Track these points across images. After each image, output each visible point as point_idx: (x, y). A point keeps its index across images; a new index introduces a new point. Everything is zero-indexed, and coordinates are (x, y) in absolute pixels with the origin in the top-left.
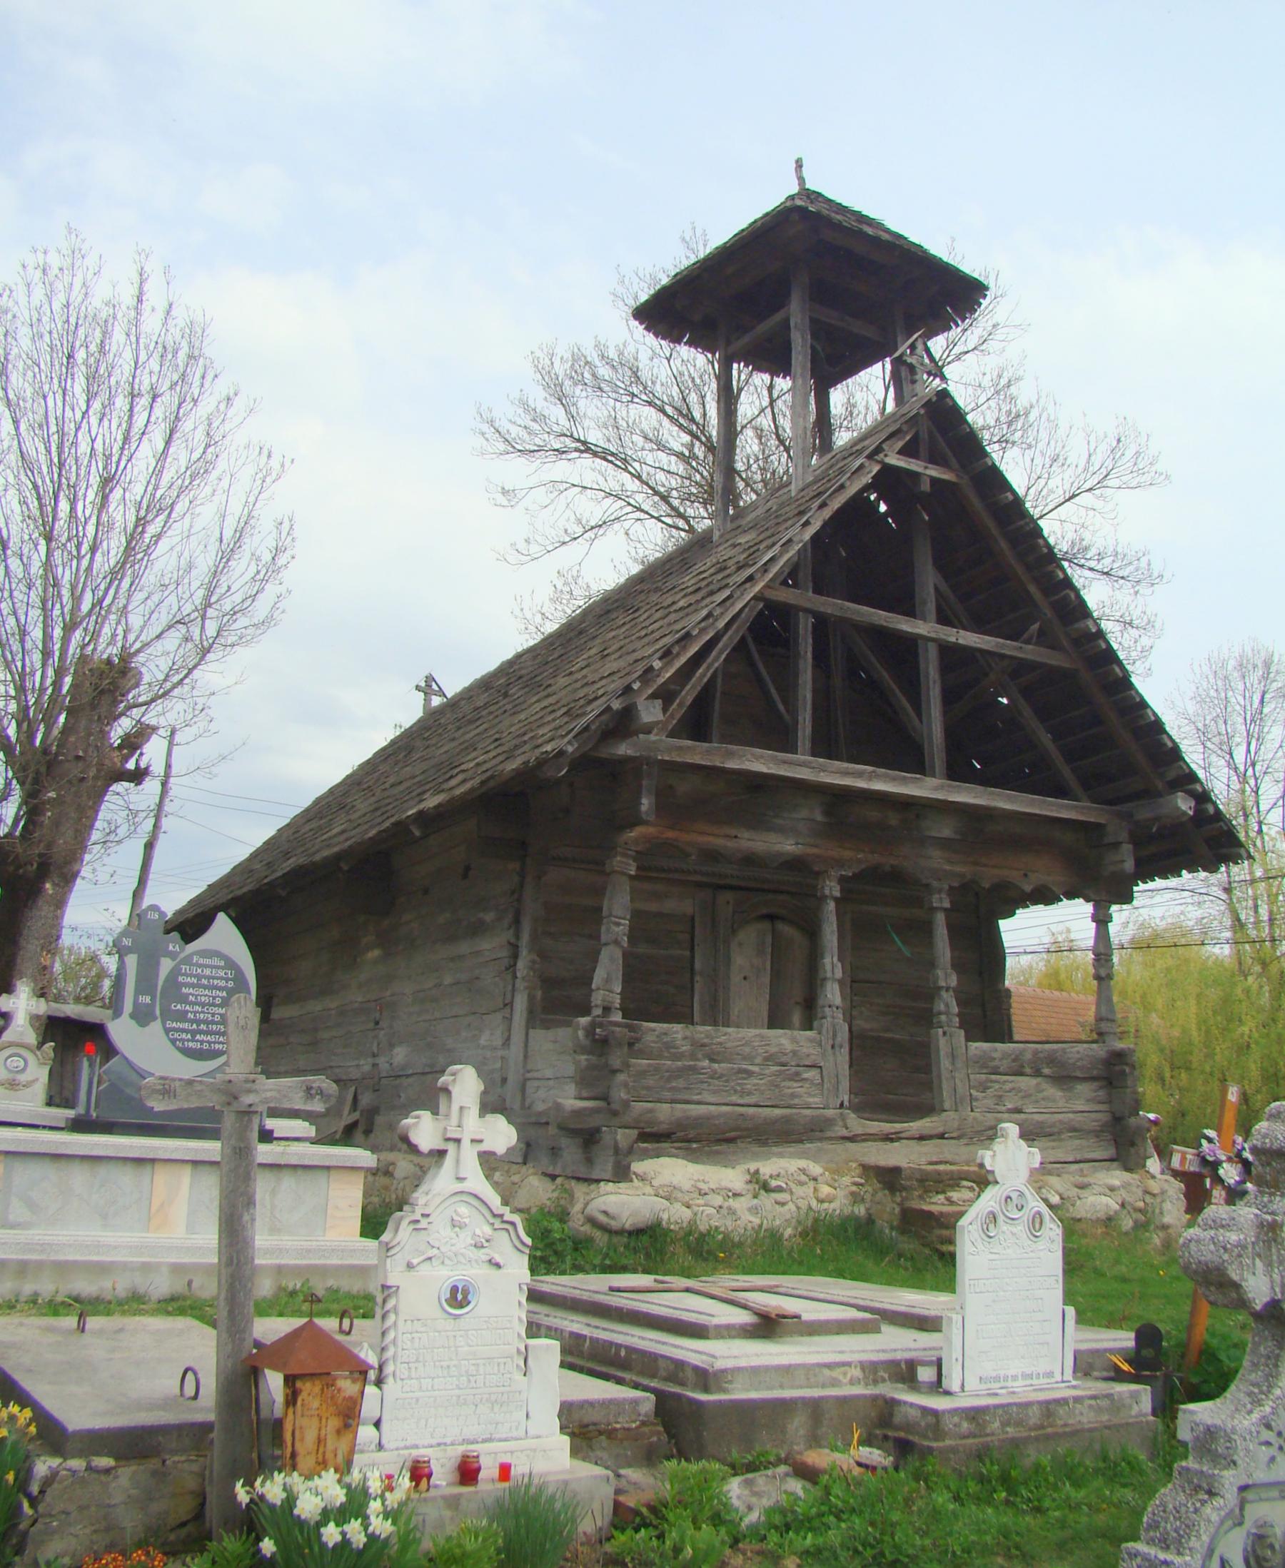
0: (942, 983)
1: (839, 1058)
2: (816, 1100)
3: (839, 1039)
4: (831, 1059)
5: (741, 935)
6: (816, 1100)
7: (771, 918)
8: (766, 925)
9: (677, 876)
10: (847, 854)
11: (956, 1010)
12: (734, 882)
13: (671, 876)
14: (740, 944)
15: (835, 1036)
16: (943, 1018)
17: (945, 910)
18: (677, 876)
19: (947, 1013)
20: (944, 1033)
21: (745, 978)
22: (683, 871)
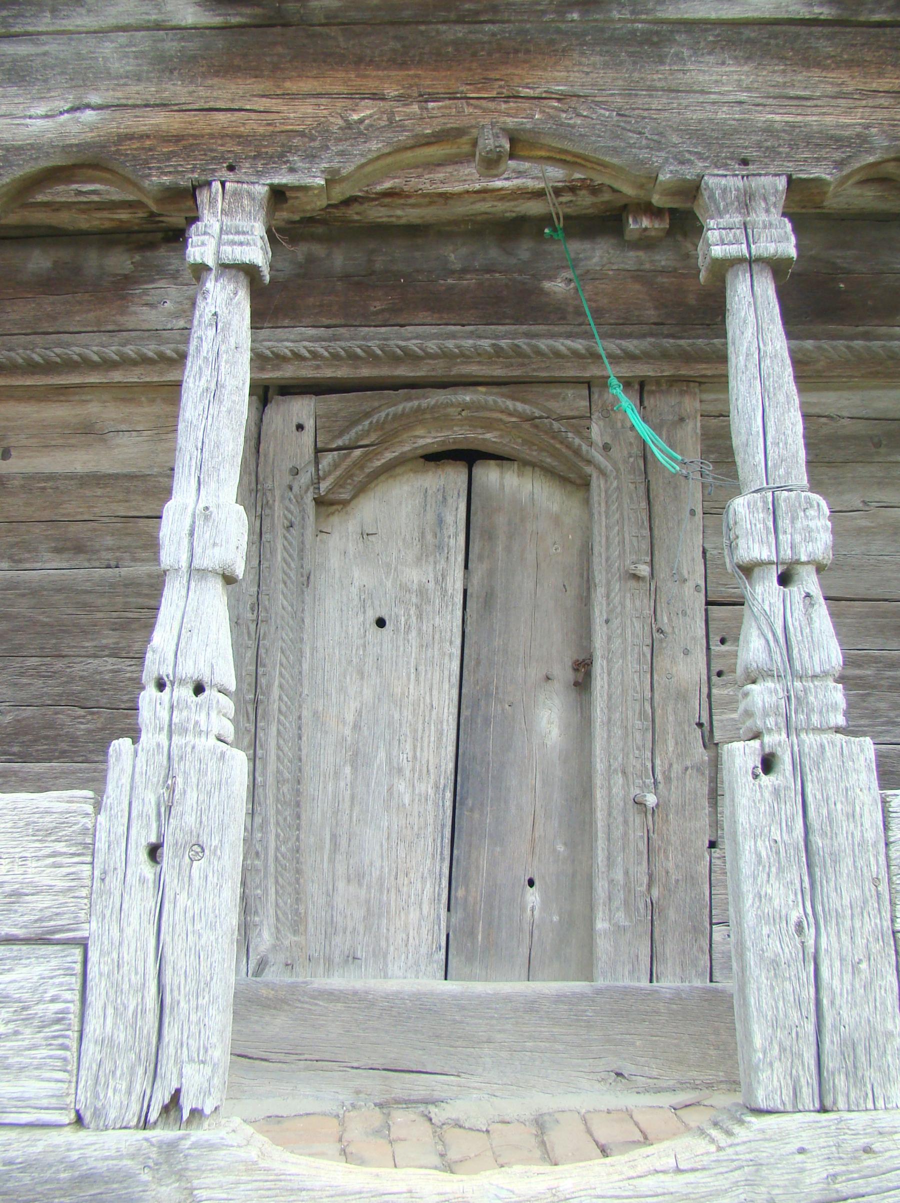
0: (754, 547)
1: (181, 902)
2: (32, 1087)
3: (187, 816)
4: (140, 904)
5: (368, 509)
6: (32, 1087)
7: (469, 457)
8: (453, 478)
9: (133, 376)
10: (300, 114)
11: (831, 654)
12: (307, 372)
13: (117, 376)
14: (365, 535)
15: (166, 809)
16: (762, 694)
17: (777, 267)
18: (133, 376)
19: (788, 669)
20: (768, 764)
21: (381, 623)
22: (145, 360)
